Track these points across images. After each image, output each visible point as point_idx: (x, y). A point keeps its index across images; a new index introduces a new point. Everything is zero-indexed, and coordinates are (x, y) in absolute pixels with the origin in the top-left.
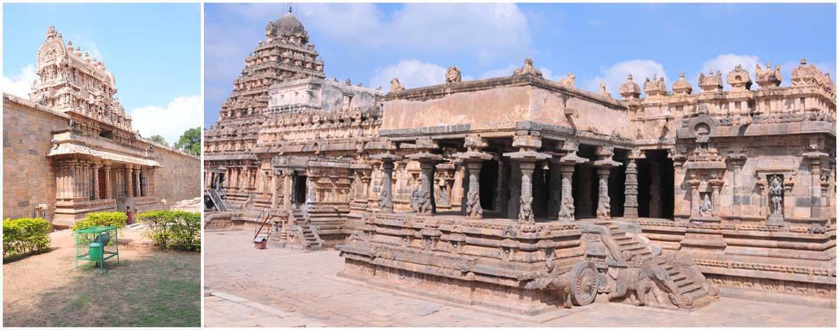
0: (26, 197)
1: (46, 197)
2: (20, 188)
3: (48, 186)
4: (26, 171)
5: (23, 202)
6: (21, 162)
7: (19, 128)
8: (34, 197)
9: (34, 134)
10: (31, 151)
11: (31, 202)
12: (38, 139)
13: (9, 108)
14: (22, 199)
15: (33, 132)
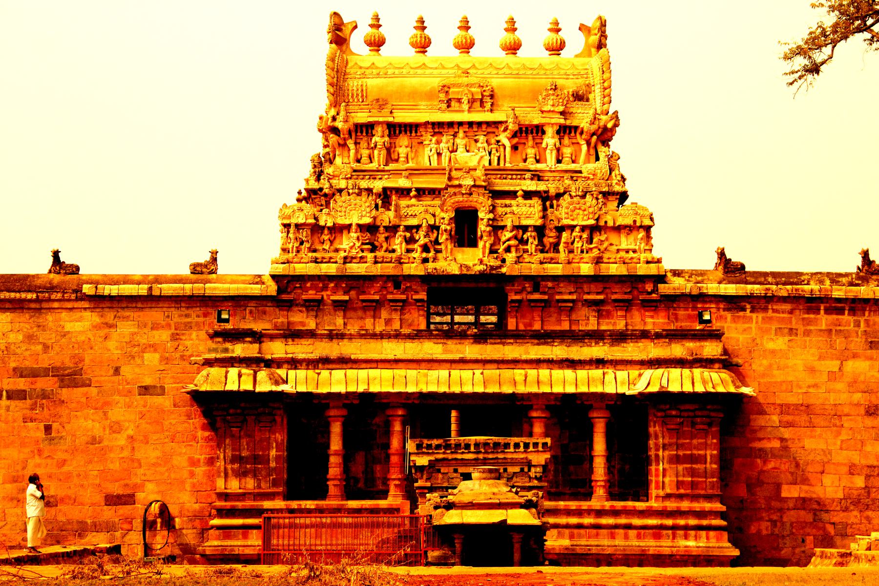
0: (126, 485)
1: (188, 487)
2: (111, 466)
4: (130, 432)
5: (119, 497)
6: (116, 414)
7: (112, 344)
8: (150, 486)
9: (155, 351)
10: (146, 388)
11: (140, 496)
12: (166, 360)
13: (85, 309)
14: (116, 489)
15: (150, 346)
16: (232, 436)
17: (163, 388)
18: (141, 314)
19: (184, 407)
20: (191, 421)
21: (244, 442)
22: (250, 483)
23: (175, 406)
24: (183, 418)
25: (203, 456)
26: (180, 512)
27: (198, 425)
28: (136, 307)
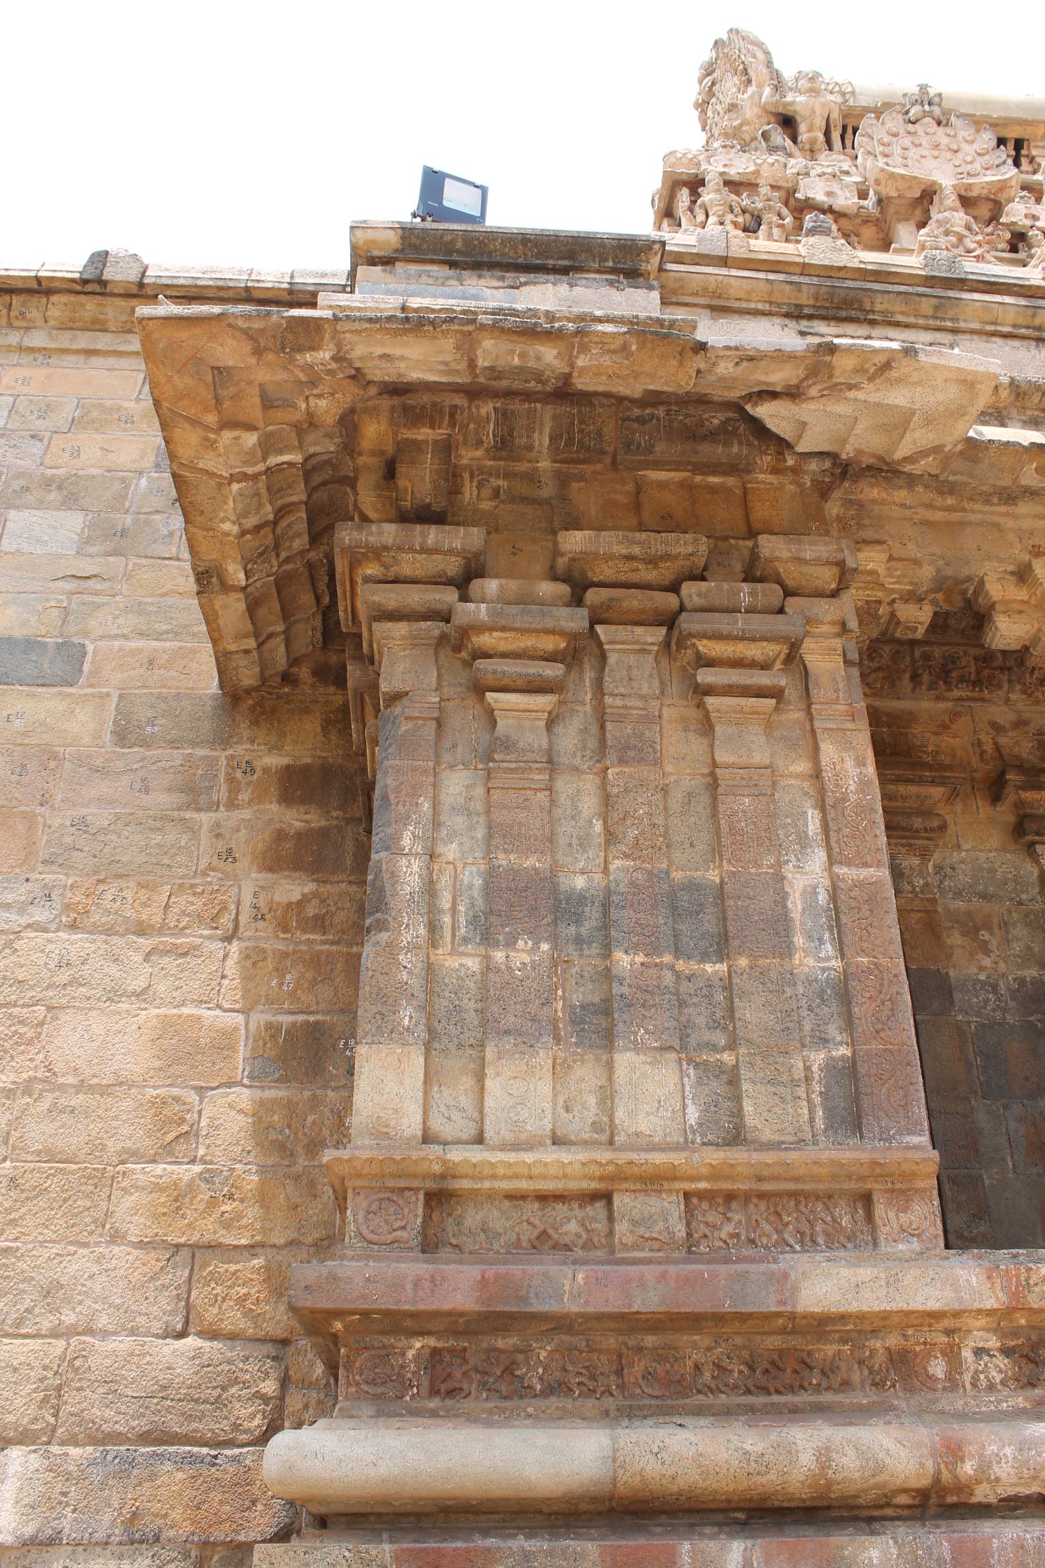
1: (132, 1212)
3: (184, 1052)
15: (47, 483)
16: (492, 751)
17: (72, 655)
18: (39, 374)
19: (174, 744)
20: (205, 818)
21: (580, 795)
22: (654, 1099)
23: (122, 736)
24: (161, 799)
25: (260, 1018)
26: (53, 1397)
27: (240, 841)
28: (21, 349)
